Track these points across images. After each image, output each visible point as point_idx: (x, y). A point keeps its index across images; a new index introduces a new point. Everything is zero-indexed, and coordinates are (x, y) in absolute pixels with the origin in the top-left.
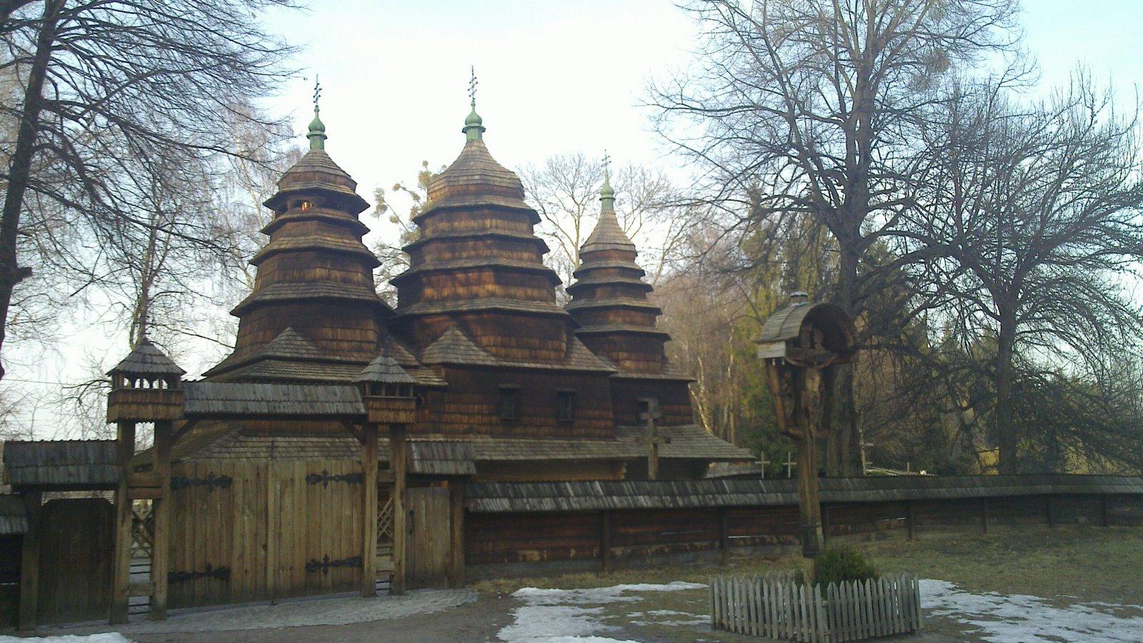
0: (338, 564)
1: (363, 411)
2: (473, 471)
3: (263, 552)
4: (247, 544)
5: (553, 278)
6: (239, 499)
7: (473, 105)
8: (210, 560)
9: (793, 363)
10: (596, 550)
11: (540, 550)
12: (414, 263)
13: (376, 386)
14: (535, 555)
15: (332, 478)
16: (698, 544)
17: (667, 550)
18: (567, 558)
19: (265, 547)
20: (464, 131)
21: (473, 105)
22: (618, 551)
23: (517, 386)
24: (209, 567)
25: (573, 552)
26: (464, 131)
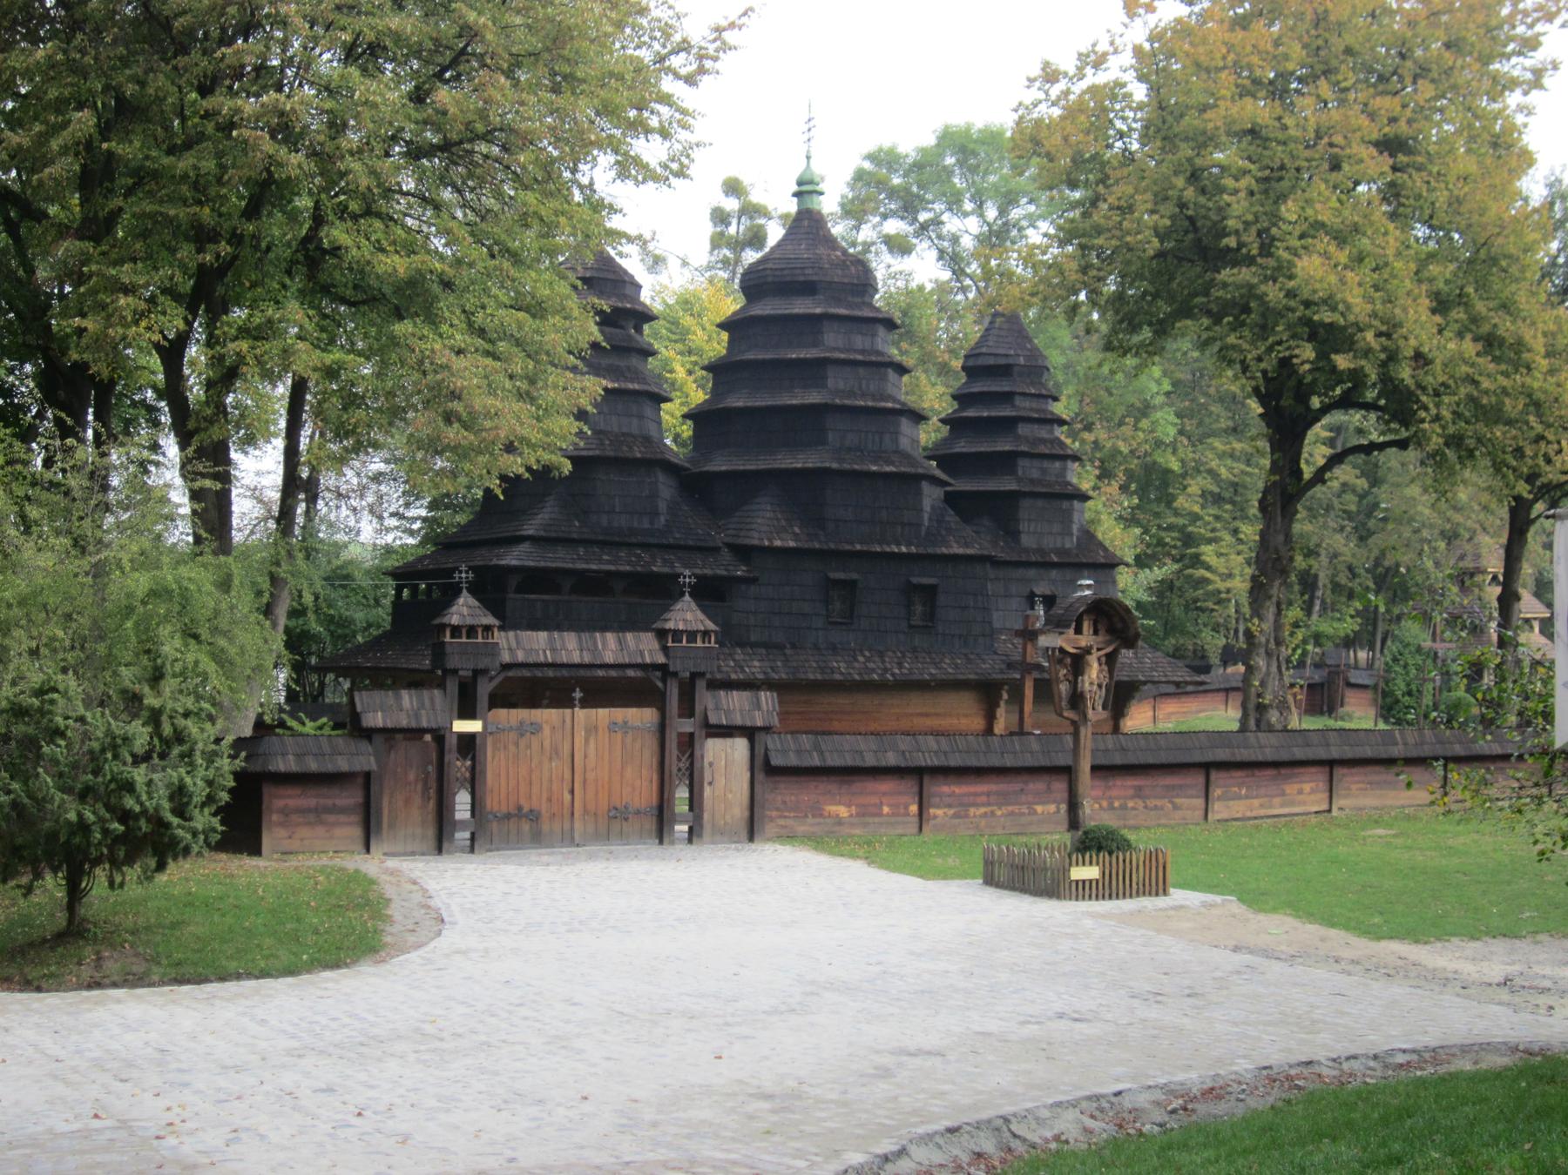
0: (638, 812)
1: (661, 659)
2: (775, 721)
3: (567, 797)
4: (555, 787)
5: (918, 417)
6: (547, 743)
7: (808, 158)
8: (523, 802)
9: (1072, 651)
10: (914, 808)
11: (849, 806)
12: (717, 393)
13: (677, 635)
14: (843, 811)
15: (633, 728)
16: (1039, 809)
17: (999, 813)
18: (880, 814)
19: (572, 792)
20: (796, 194)
21: (808, 158)
22: (939, 812)
23: (854, 576)
24: (520, 808)
25: (886, 809)
26: (796, 194)
